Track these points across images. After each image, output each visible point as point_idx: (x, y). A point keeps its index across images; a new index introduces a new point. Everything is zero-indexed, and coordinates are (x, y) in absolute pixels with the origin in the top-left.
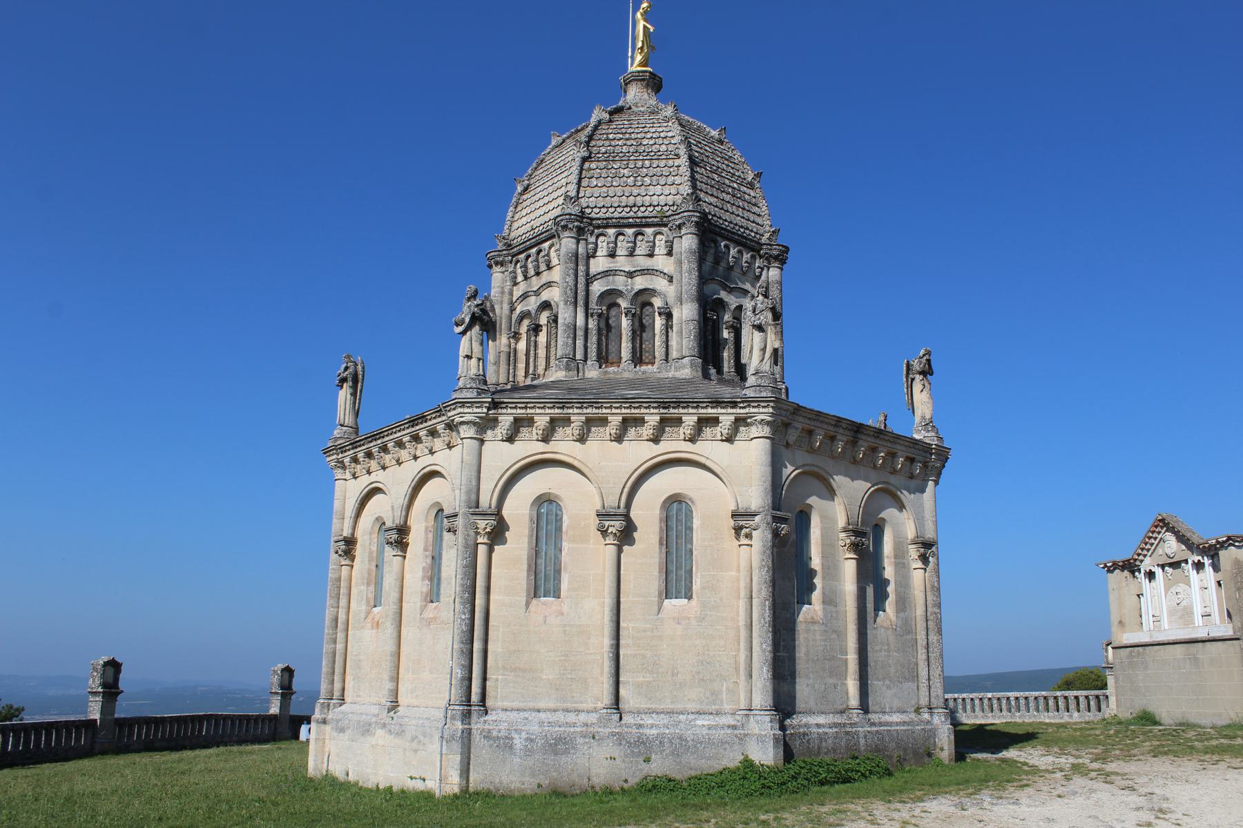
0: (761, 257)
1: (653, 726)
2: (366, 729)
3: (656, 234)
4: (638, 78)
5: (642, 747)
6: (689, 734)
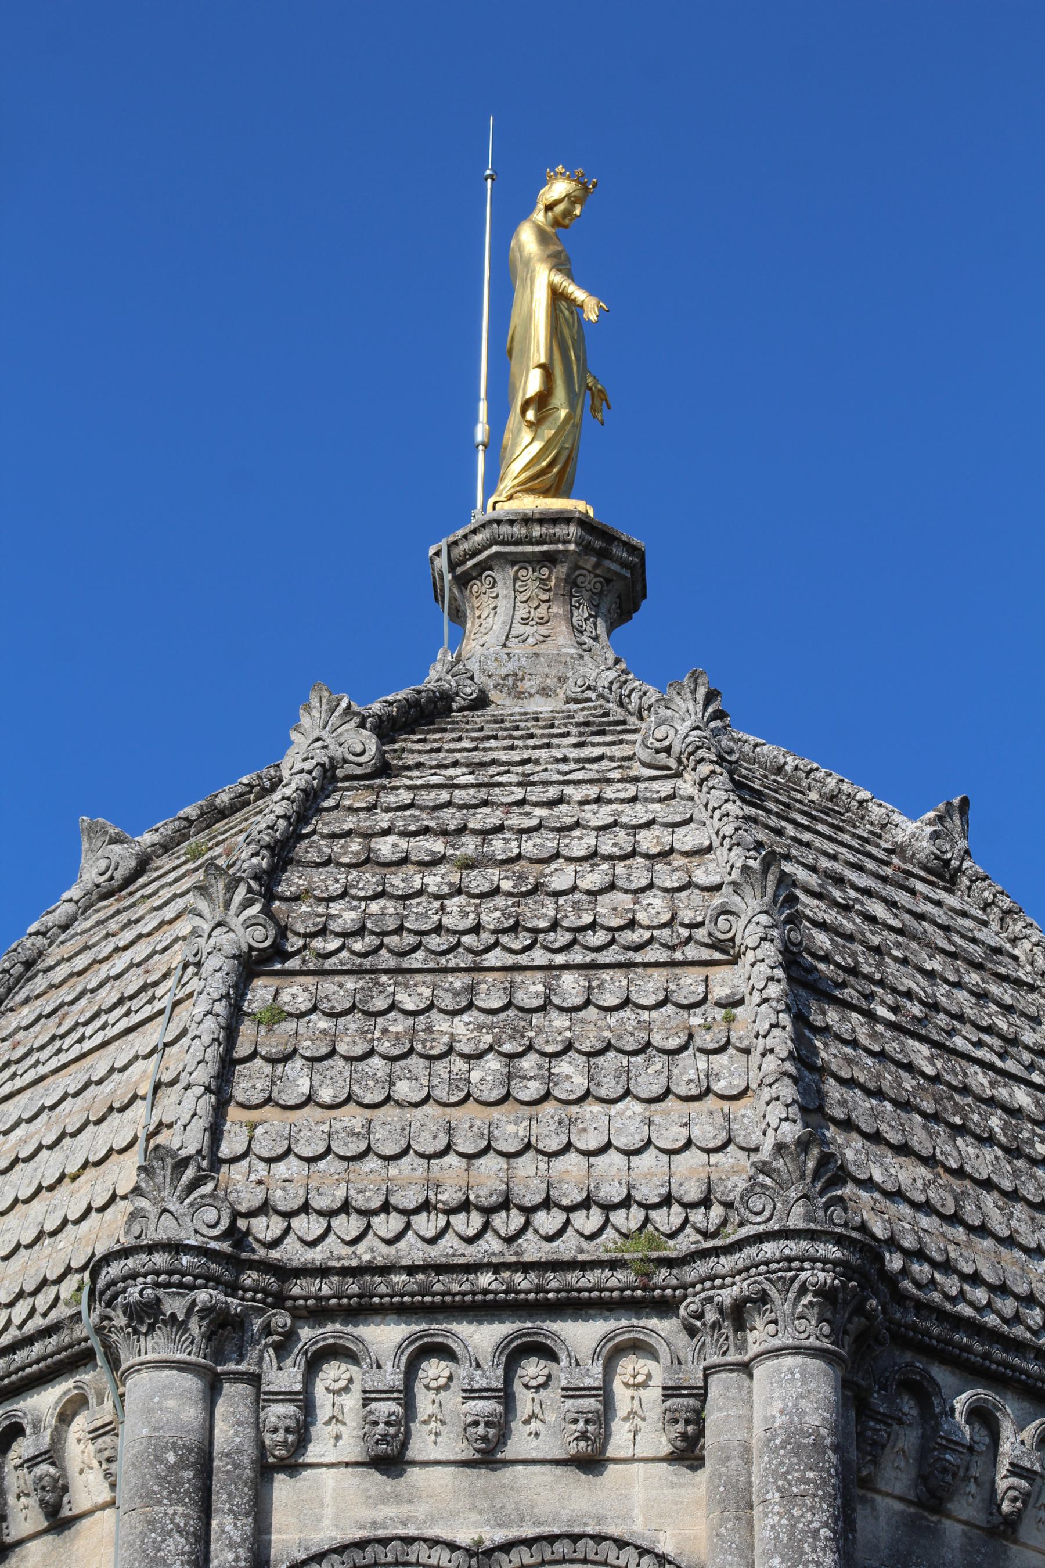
3: (614, 1353)
4: (524, 550)
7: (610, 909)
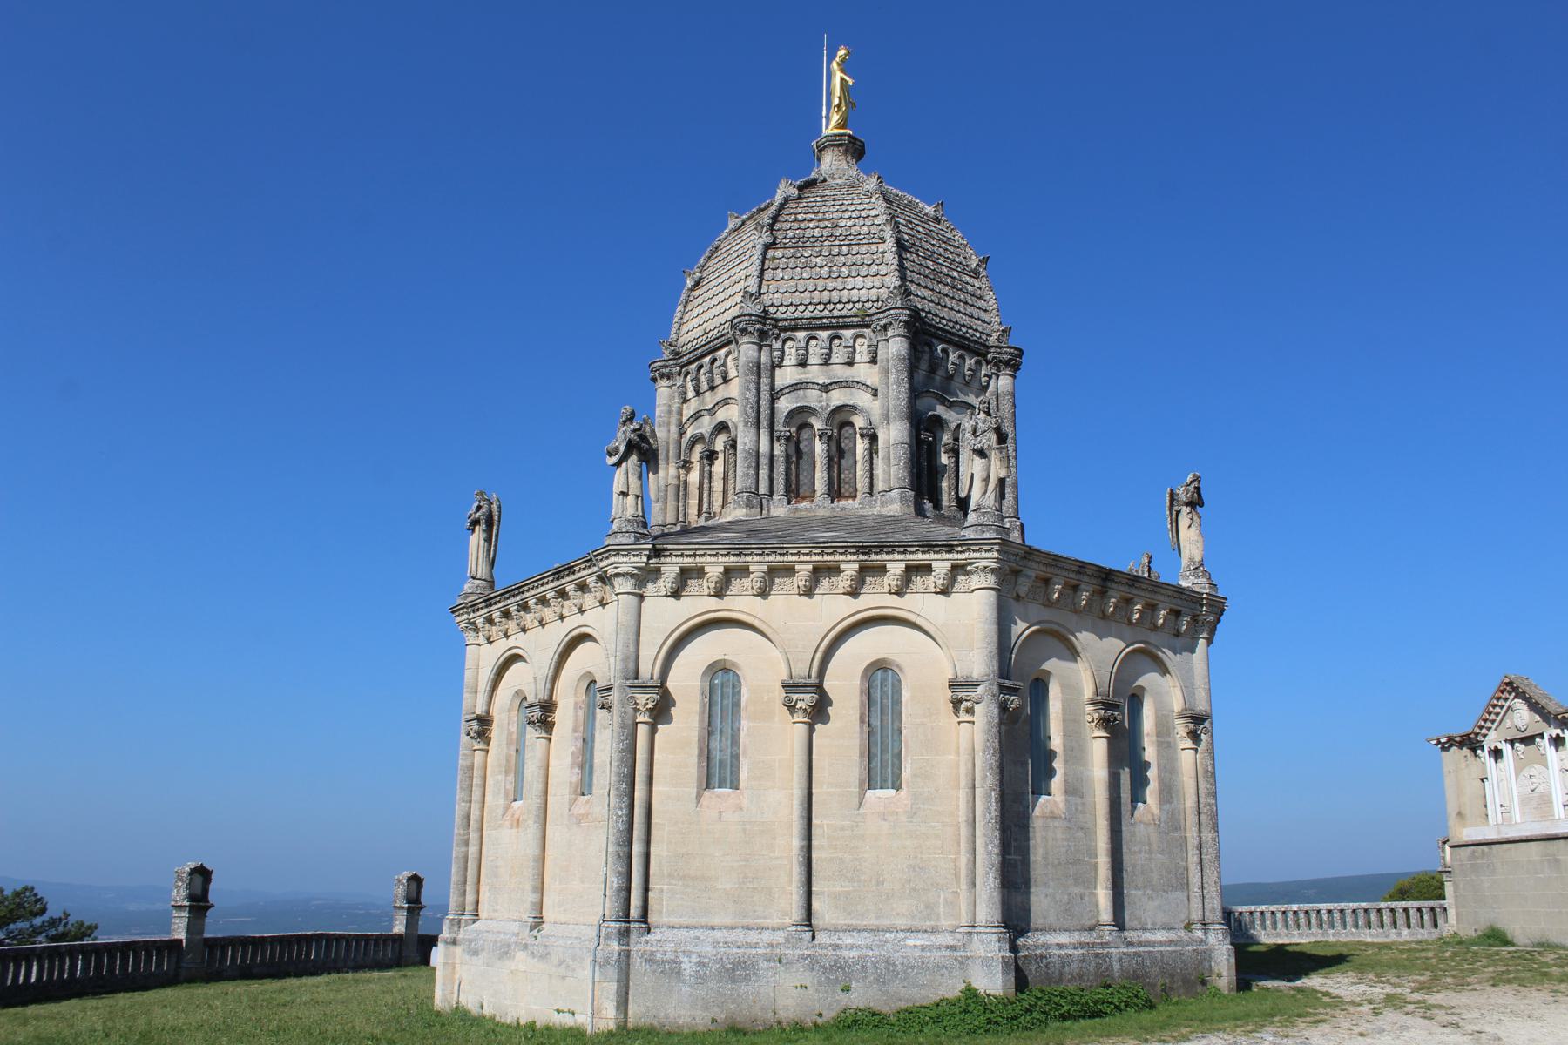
0: (988, 363)
1: (854, 947)
2: (504, 952)
3: (856, 338)
4: (834, 143)
5: (839, 973)
6: (897, 957)
7: (854, 231)
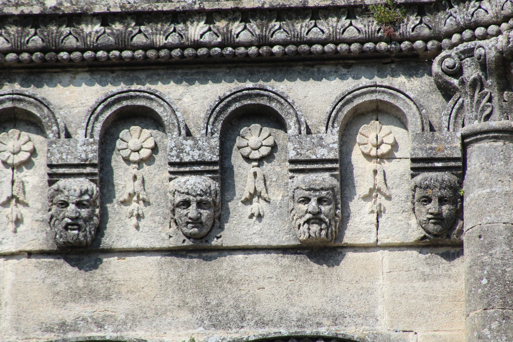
3: (352, 118)
